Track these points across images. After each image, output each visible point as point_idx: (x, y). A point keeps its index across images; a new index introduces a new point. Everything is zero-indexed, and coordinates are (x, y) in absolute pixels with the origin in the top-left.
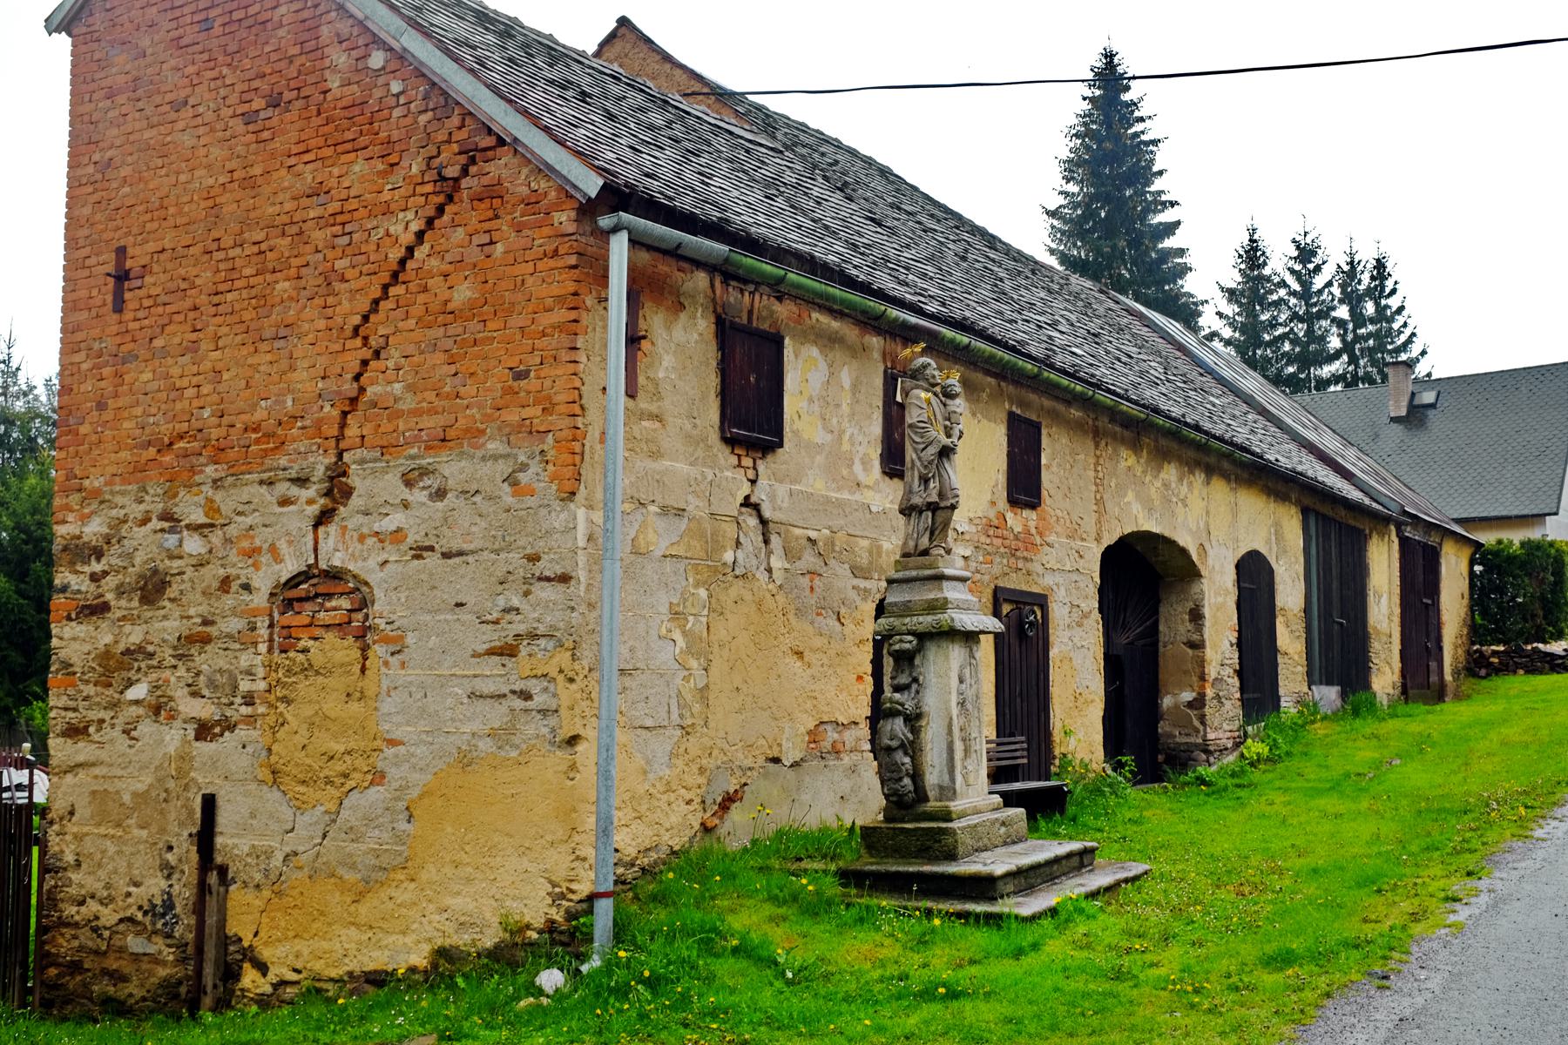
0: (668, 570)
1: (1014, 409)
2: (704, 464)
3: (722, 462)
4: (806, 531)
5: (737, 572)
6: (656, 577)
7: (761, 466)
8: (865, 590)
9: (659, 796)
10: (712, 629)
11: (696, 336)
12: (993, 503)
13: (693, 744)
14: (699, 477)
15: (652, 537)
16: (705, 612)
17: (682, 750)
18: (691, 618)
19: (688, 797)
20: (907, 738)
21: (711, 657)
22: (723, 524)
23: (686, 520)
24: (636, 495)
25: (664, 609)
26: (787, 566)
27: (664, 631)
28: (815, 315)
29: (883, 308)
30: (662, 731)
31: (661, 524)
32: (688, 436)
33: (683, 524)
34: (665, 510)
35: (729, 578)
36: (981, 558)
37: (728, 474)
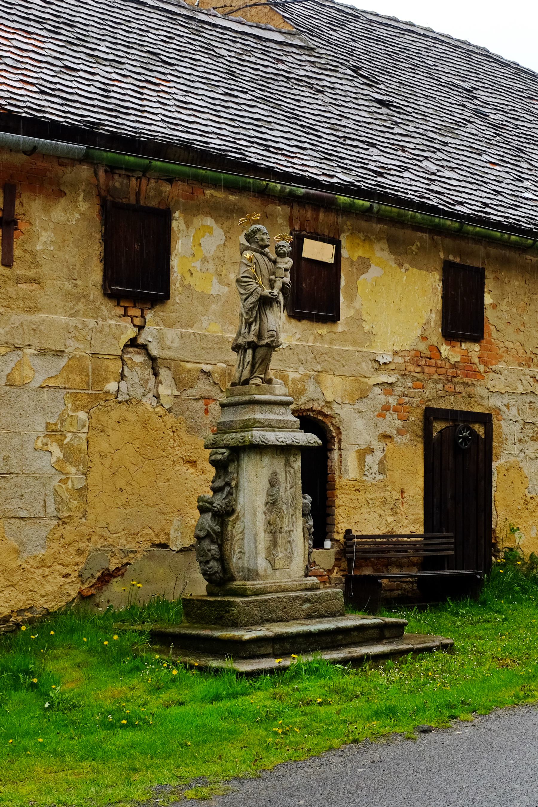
0: (46, 397)
1: (451, 258)
2: (86, 315)
3: (106, 313)
4: (199, 365)
5: (120, 399)
6: (32, 404)
7: (149, 316)
9: (32, 570)
10: (91, 443)
11: (77, 215)
12: (424, 338)
13: (68, 531)
14: (80, 326)
15: (27, 372)
16: (85, 430)
17: (58, 535)
18: (69, 435)
19: (65, 571)
20: (213, 530)
21: (90, 464)
22: (106, 362)
23: (65, 360)
24: (11, 341)
25: (41, 428)
26: (178, 393)
27: (39, 444)
28: (208, 192)
29: (265, 183)
31: (38, 362)
32: (68, 294)
33: (63, 362)
34: (42, 352)
35: (111, 403)
36: (410, 384)
37: (113, 322)
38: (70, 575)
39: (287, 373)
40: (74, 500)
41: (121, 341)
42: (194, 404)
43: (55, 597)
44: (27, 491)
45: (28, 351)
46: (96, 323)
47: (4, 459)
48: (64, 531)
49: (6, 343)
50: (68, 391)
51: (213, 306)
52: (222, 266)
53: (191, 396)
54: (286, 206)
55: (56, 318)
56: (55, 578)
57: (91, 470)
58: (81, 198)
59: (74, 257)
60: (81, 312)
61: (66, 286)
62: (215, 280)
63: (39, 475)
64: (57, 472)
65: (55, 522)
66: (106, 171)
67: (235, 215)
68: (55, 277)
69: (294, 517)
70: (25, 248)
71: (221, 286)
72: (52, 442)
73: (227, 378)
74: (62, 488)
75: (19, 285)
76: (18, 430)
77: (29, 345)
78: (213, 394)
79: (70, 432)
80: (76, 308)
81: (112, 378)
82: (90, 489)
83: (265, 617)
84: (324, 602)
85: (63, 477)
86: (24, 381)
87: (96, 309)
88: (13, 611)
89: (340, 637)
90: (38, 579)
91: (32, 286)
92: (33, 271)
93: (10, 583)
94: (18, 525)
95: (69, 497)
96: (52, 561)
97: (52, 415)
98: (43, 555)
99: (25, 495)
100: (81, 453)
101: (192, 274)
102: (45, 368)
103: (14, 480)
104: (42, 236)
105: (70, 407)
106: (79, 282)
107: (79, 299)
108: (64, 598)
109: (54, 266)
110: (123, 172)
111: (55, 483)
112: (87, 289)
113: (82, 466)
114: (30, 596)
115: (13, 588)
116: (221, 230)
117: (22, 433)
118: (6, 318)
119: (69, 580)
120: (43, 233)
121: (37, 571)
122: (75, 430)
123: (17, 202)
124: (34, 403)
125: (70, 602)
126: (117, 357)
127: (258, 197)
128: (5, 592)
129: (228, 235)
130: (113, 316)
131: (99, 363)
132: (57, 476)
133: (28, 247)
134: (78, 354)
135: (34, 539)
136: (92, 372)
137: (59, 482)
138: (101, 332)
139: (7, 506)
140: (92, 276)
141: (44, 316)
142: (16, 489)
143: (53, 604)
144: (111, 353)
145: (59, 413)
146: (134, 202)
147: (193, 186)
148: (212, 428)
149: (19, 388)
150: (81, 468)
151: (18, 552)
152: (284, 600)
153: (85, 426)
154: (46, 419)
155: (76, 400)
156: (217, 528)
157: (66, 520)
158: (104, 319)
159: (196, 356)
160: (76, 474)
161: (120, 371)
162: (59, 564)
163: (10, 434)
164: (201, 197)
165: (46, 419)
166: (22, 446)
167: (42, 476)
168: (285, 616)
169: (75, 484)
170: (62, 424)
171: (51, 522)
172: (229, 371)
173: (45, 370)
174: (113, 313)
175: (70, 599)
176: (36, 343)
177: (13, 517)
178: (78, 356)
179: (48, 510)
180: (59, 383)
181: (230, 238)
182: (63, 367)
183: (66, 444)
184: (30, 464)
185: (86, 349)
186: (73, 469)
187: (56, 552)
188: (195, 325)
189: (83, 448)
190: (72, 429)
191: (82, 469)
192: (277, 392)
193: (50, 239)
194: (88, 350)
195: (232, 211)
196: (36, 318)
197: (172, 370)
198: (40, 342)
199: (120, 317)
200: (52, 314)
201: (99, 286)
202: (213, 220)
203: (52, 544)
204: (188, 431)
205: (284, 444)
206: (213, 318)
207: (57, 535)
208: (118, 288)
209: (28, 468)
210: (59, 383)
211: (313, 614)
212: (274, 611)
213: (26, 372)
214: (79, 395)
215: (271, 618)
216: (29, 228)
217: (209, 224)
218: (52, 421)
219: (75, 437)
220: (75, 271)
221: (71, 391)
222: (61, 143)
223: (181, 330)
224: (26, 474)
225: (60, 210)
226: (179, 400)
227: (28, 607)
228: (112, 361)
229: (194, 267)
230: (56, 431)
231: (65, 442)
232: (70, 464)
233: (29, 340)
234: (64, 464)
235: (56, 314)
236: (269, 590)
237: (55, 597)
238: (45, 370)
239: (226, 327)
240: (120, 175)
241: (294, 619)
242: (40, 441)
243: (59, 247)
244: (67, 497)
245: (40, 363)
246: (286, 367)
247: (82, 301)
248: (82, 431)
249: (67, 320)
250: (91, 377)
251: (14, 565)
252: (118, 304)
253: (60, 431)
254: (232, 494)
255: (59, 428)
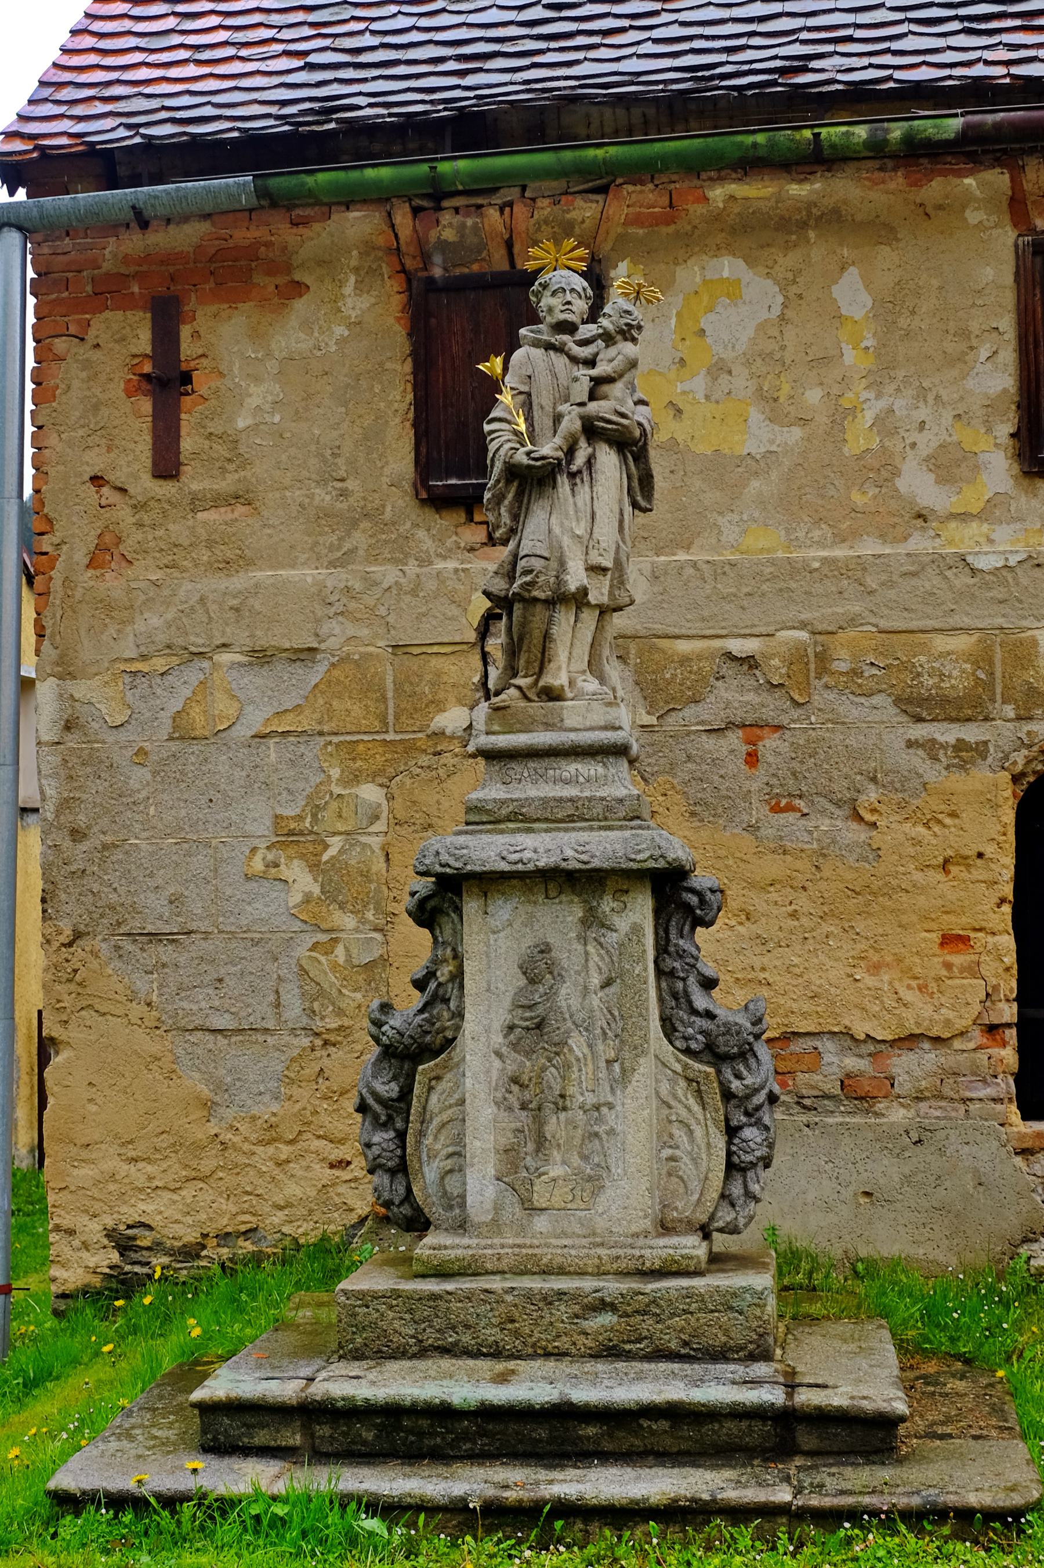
0: (273, 756)
2: (374, 558)
4: (717, 643)
6: (239, 774)
8: (961, 746)
9: (246, 1147)
10: (395, 857)
11: (340, 331)
14: (358, 586)
15: (224, 706)
18: (336, 843)
19: (337, 1153)
22: (434, 662)
23: (322, 668)
24: (180, 641)
25: (262, 828)
26: (652, 720)
27: (258, 865)
28: (718, 193)
29: (807, 134)
30: (261, 1038)
31: (254, 681)
33: (317, 673)
35: (447, 759)
37: (451, 565)
38: (349, 1163)
39: (1030, 633)
40: (355, 991)
41: (471, 608)
42: (709, 743)
43: (311, 1212)
44: (233, 969)
45: (225, 658)
46: (400, 574)
47: (171, 902)
48: (326, 1061)
49: (169, 647)
50: (329, 738)
51: (755, 484)
52: (779, 375)
53: (698, 724)
54: (998, 170)
55: (293, 576)
56: (308, 1168)
57: (396, 920)
58: (348, 289)
59: (336, 426)
60: (361, 552)
61: (317, 499)
62: (755, 415)
63: (258, 936)
64: (304, 927)
65: (306, 1042)
66: (416, 211)
67: (812, 234)
68: (287, 481)
69: (617, 1067)
70: (209, 430)
71: (777, 428)
72: (290, 858)
73: (812, 666)
74: (319, 962)
75: (199, 514)
76: (205, 835)
77: (224, 645)
78: (769, 714)
79: (340, 833)
80: (347, 546)
81: (452, 699)
82: (396, 964)
83: (430, 1337)
84: (673, 1315)
85: (323, 937)
86: (215, 726)
87: (401, 540)
88: (207, 1235)
89: (591, 1431)
90: (264, 1169)
91: (233, 511)
92: (231, 478)
93: (194, 1174)
94: (210, 1046)
95: (338, 984)
96: (297, 1129)
97: (290, 798)
98: (274, 1114)
99: (227, 979)
100: (370, 881)
101: (679, 411)
102: (270, 693)
103: (198, 946)
104: (250, 395)
105: (337, 776)
106: (351, 484)
107: (354, 524)
108: (336, 1215)
109: (284, 457)
110: (459, 201)
111: (301, 951)
112: (376, 495)
113: (372, 912)
114: (246, 1206)
115: (202, 1185)
116: (769, 282)
117: (214, 842)
118: (166, 592)
119: (346, 1175)
120: (253, 389)
121: (259, 1149)
122: (350, 828)
123: (185, 331)
124: (244, 774)
125: (353, 1226)
126: (465, 647)
127: (895, 169)
128: (184, 1193)
129: (794, 290)
130: (450, 550)
131: (415, 668)
132: (307, 936)
133: (213, 427)
134: (356, 651)
135: (252, 1077)
136: (396, 690)
137: (310, 950)
138: (414, 593)
139: (185, 1004)
140: (387, 463)
141: (262, 575)
142: (204, 967)
143: (305, 1227)
144: (446, 640)
145: (309, 790)
146: (505, 267)
147: (672, 186)
148: (773, 802)
149: (204, 742)
150: (370, 915)
151: (209, 1107)
152: (509, 1298)
153: (377, 818)
154: (273, 808)
155: (354, 759)
156: (390, 1089)
157: (332, 1038)
158: (425, 561)
159: (703, 620)
160: (357, 930)
161: (476, 679)
162: (319, 1137)
163: (186, 846)
164: (698, 210)
165: (273, 808)
166: (216, 871)
167: (269, 936)
168: (510, 1343)
169: (354, 952)
170: (314, 816)
171: (296, 1042)
172: (819, 649)
173: (270, 698)
174: (449, 543)
175: (353, 1218)
176: (242, 638)
177: (196, 1029)
178: (356, 657)
179: (287, 1015)
180: (305, 722)
181: (800, 296)
182: (316, 686)
183: (326, 862)
184: (236, 911)
185: (376, 635)
186: (347, 920)
187: (304, 1109)
188: (698, 542)
189: (374, 869)
190: (340, 827)
191: (372, 918)
192: (568, 723)
193: (270, 398)
194: (382, 638)
195: (803, 225)
196: (238, 582)
197: (632, 662)
198: (252, 636)
199: (472, 550)
200: (283, 568)
201: (407, 486)
202: (740, 263)
203: (295, 1091)
204: (693, 814)
205: (530, 867)
206: (756, 514)
207: (307, 1071)
208: (453, 481)
209: (232, 919)
210: (305, 722)
211: (628, 1347)
212: (467, 1327)
213: (221, 707)
214: (361, 747)
215: (456, 1344)
216: (219, 383)
217: (726, 274)
218: (289, 812)
219: (352, 845)
220: (340, 461)
221: (335, 739)
222: (190, 184)
223: (656, 559)
224: (227, 933)
225: (293, 328)
226: (656, 736)
227: (243, 1228)
228: (451, 657)
229: (684, 393)
230: (301, 833)
231: (325, 857)
232: (340, 908)
233: (224, 632)
234: (324, 909)
235: (293, 567)
236: (489, 1266)
237: (311, 1212)
238: (270, 698)
239: (801, 534)
240: (457, 210)
241: (547, 1355)
242: (258, 858)
243: (297, 412)
244: (332, 984)
245: (259, 681)
246: (1025, 618)
247: (362, 526)
248: (370, 830)
249: (321, 577)
250: (391, 704)
251: (200, 1133)
252: (470, 519)
253: (311, 832)
254: (446, 1001)
255: (308, 825)
